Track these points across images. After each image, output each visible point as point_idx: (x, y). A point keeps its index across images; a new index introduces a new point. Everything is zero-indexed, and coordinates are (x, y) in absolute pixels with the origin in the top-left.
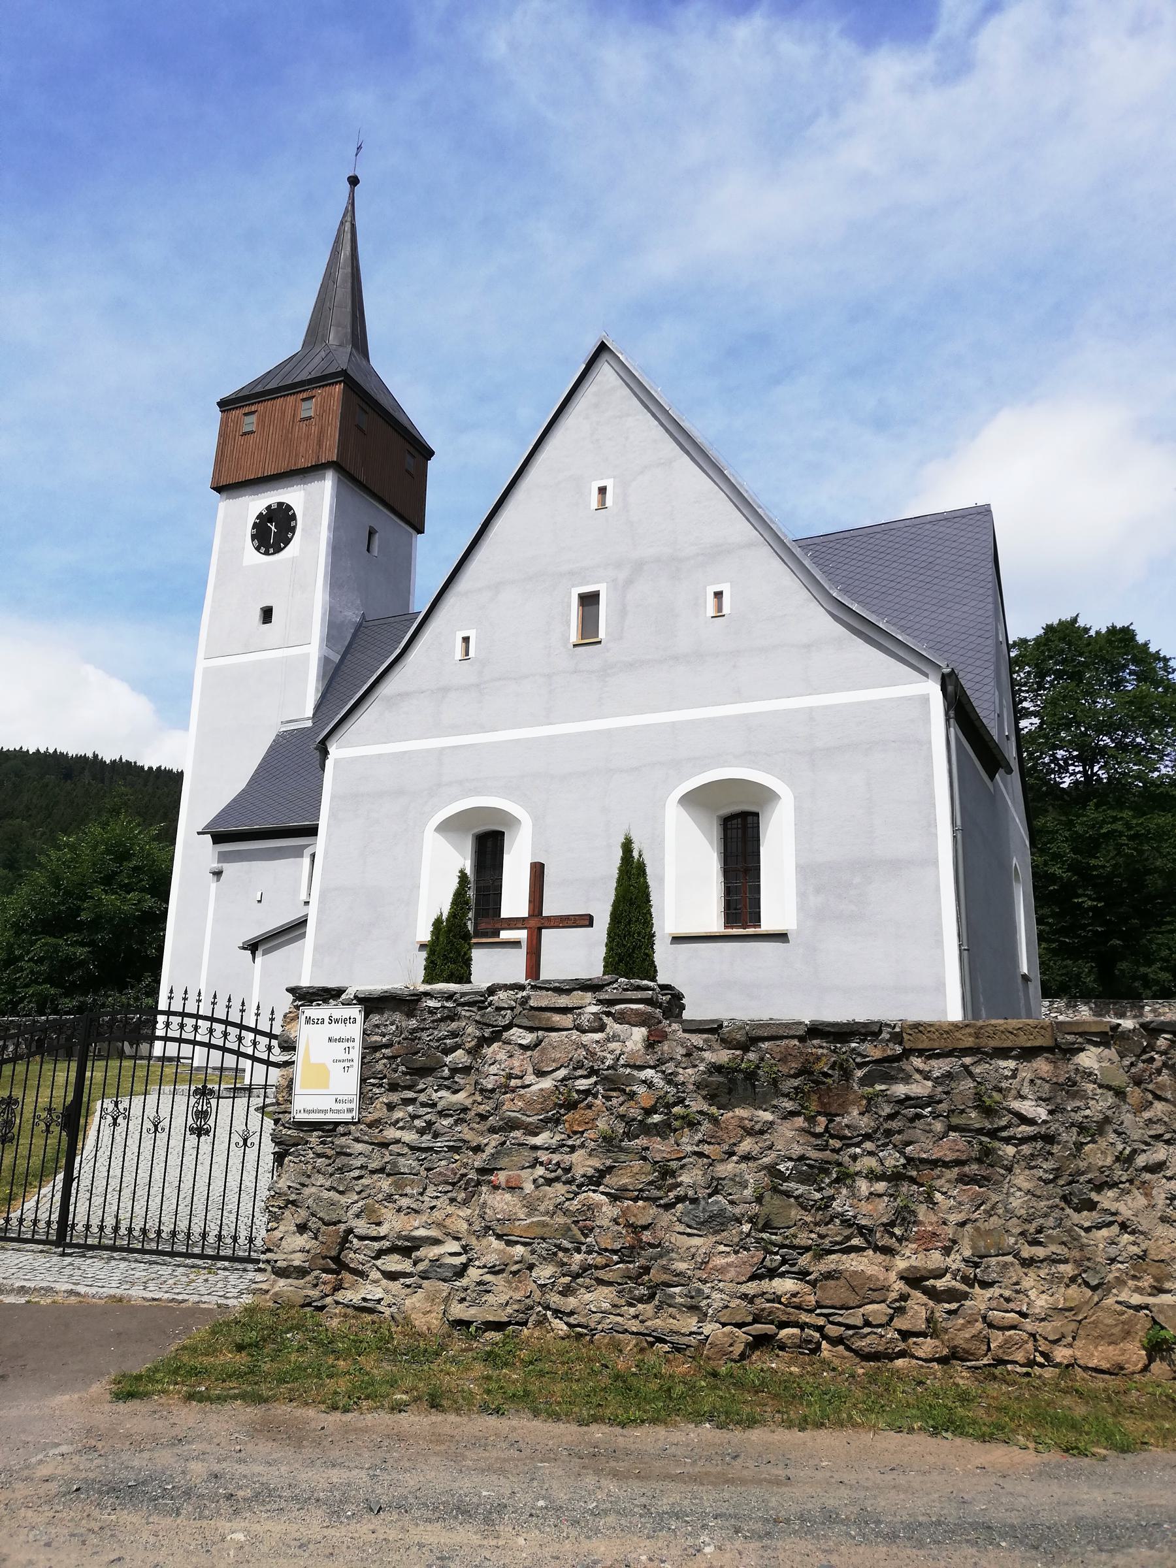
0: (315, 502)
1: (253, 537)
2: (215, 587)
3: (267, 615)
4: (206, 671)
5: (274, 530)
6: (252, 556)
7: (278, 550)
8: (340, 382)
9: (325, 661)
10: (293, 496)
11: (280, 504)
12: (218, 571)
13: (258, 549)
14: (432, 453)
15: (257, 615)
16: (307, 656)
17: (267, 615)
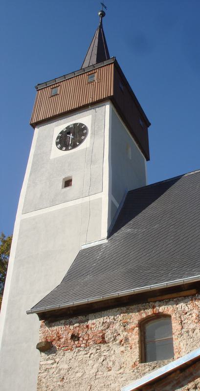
0: (99, 122)
1: (57, 143)
2: (31, 174)
3: (68, 183)
4: (22, 221)
5: (71, 138)
6: (57, 153)
7: (74, 146)
8: (112, 63)
9: (112, 206)
10: (85, 119)
11: (75, 125)
12: (33, 164)
13: (61, 149)
14: (150, 124)
15: (61, 184)
16: (101, 198)
17: (68, 183)
